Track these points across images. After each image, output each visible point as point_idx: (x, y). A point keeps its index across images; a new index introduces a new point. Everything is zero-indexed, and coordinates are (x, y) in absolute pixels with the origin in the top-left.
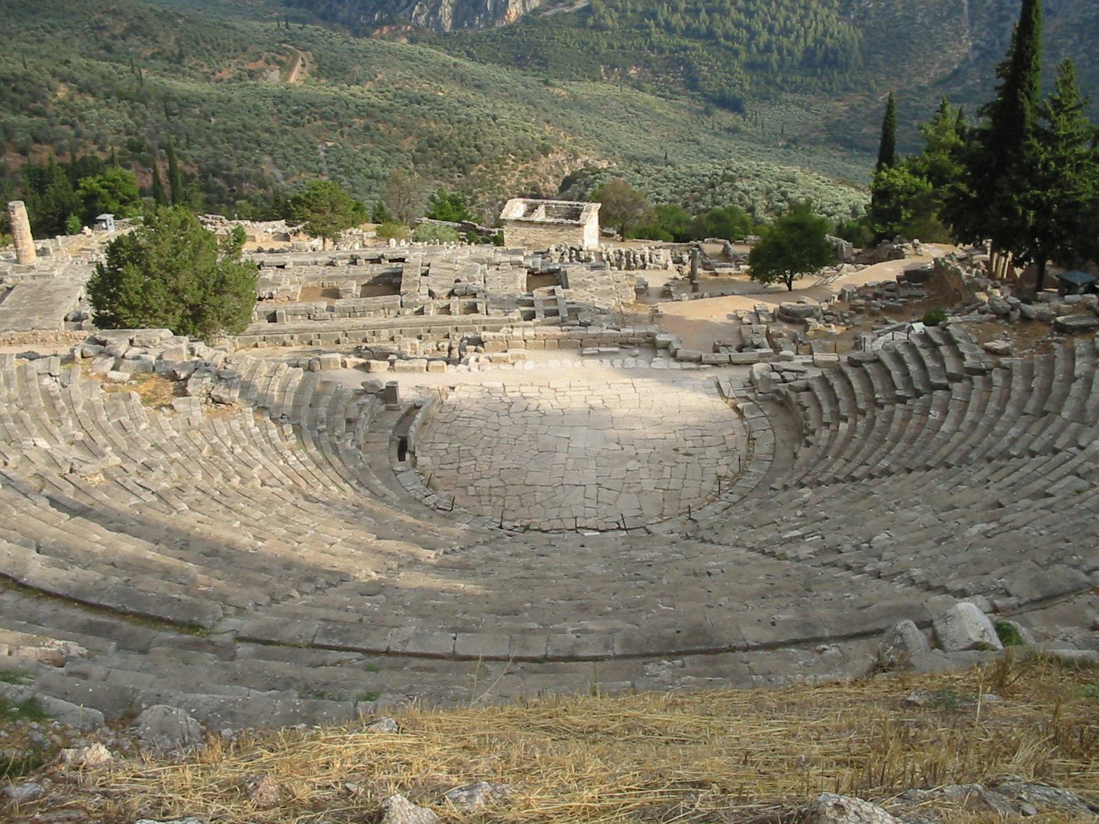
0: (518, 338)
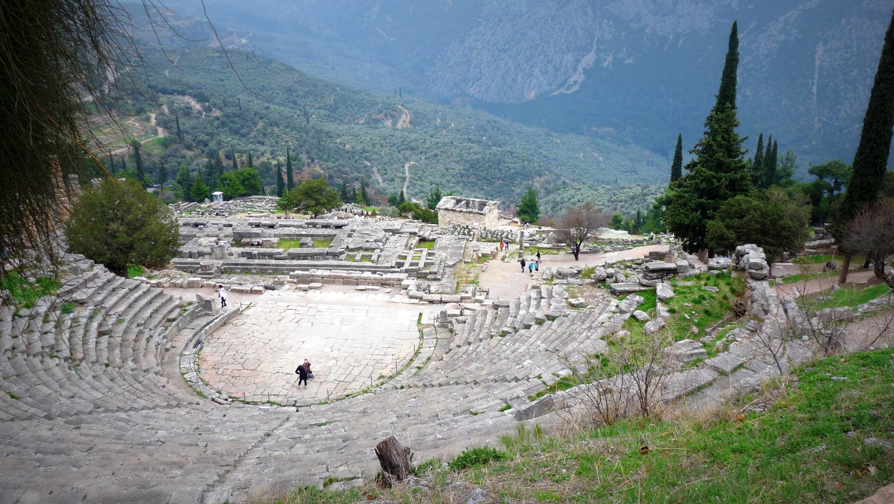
0: (318, 276)
